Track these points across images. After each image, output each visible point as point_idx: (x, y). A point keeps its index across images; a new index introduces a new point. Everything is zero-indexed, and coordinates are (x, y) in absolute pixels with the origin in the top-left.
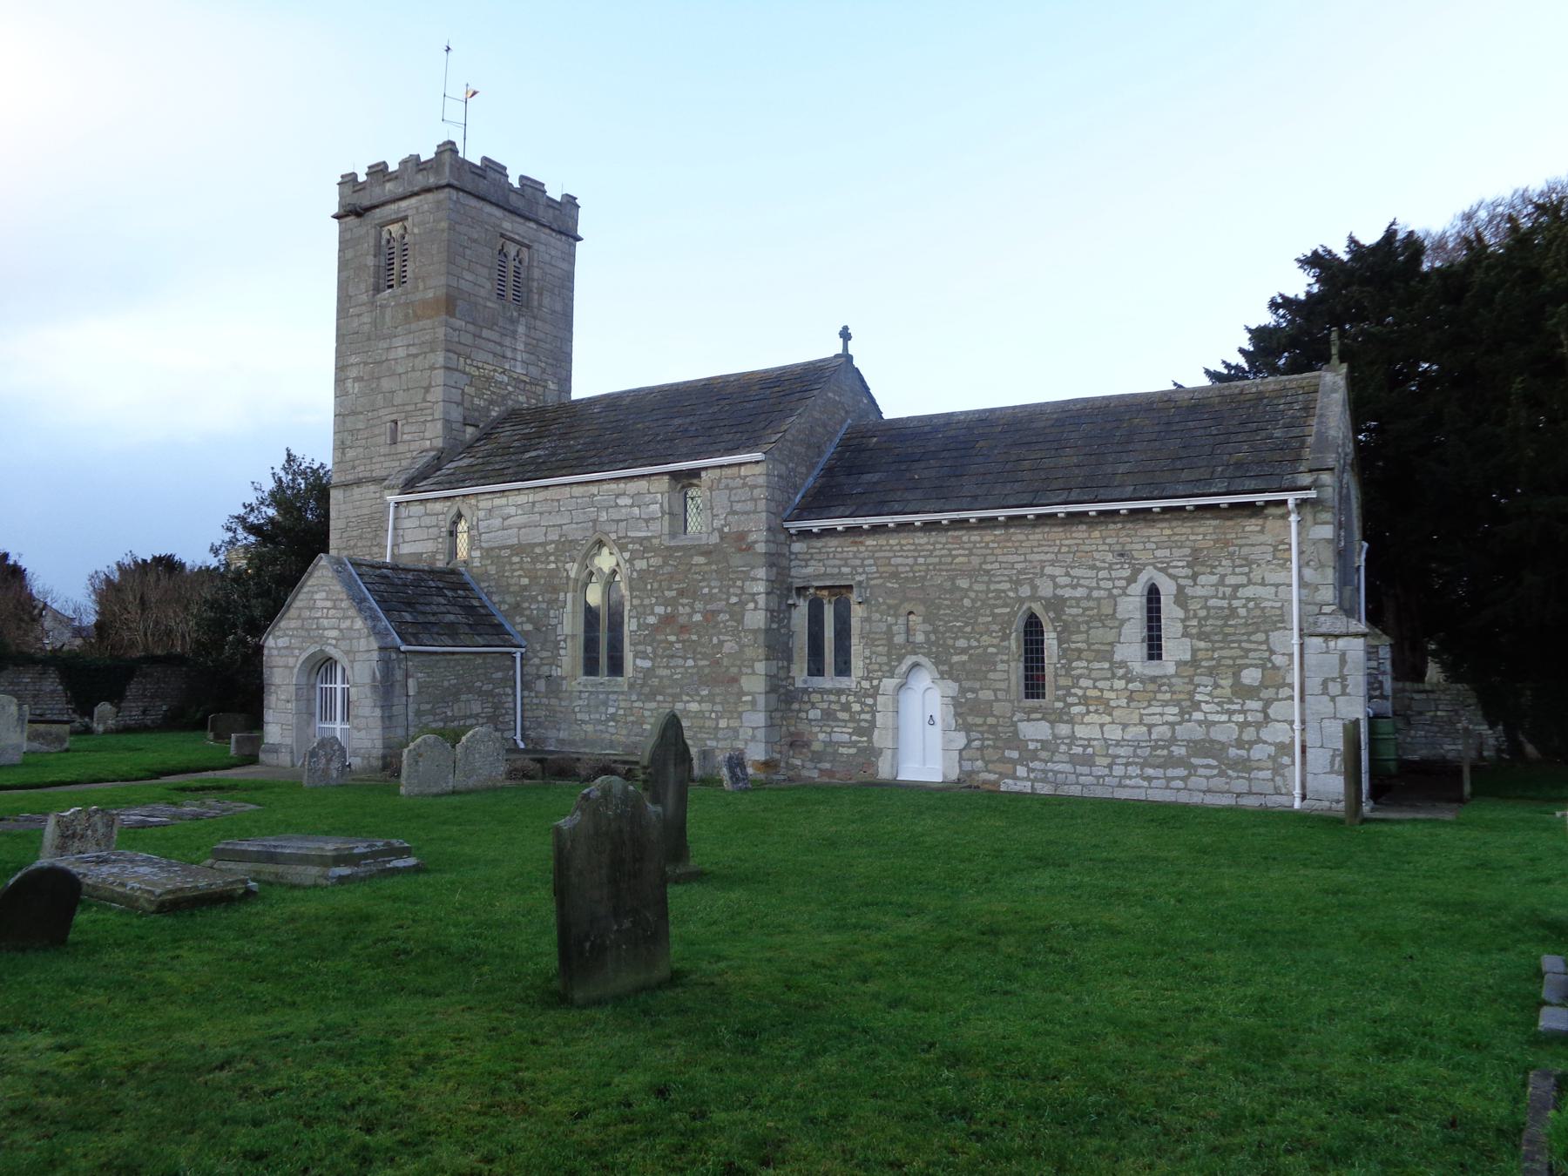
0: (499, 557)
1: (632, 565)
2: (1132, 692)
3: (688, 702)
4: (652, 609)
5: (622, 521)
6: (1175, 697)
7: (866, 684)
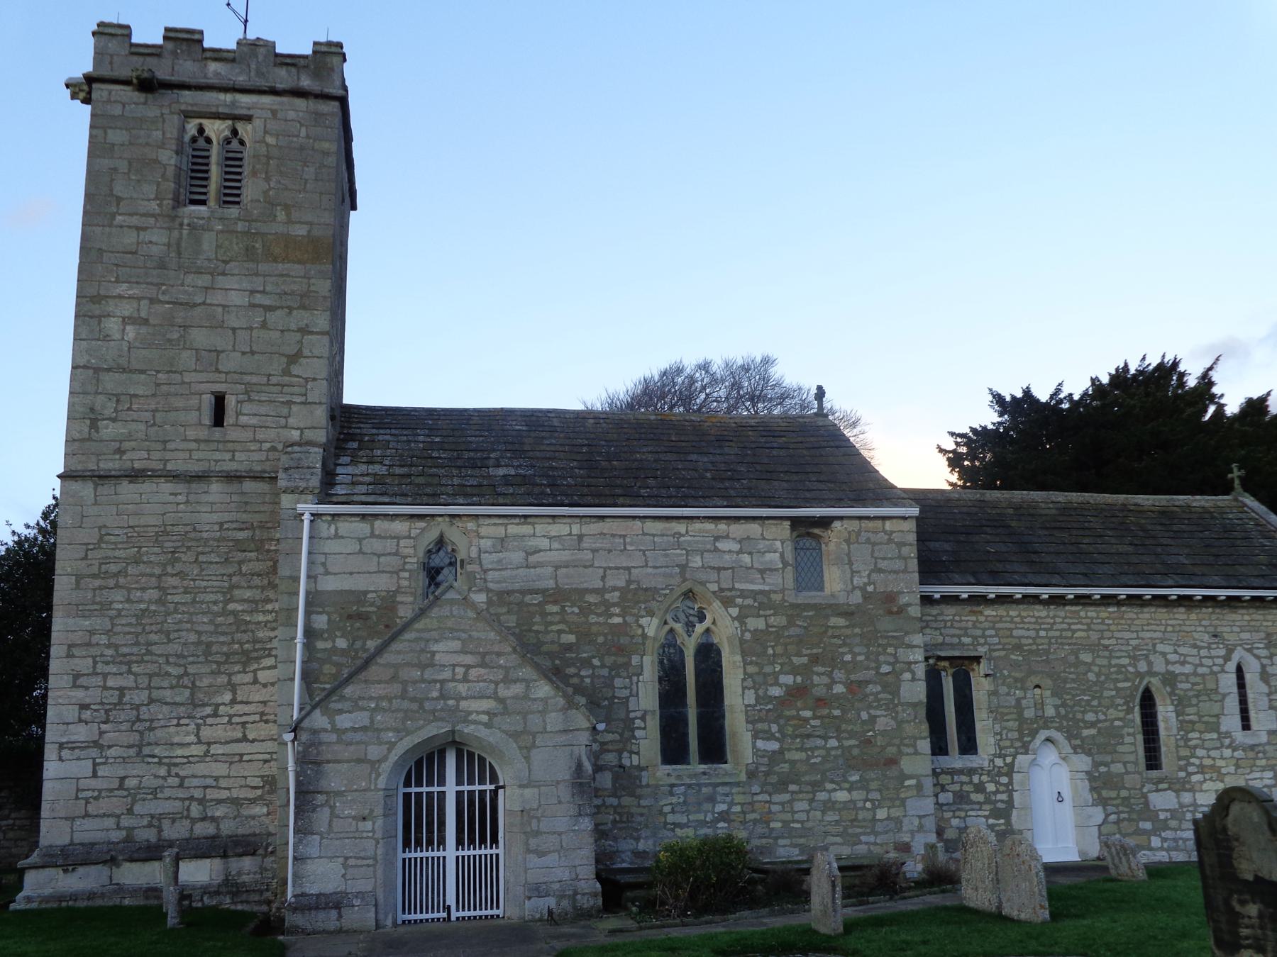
0: (521, 604)
1: (743, 623)
2: (1238, 759)
3: (835, 790)
4: (777, 679)
5: (725, 569)
6: (1269, 762)
7: (999, 762)
